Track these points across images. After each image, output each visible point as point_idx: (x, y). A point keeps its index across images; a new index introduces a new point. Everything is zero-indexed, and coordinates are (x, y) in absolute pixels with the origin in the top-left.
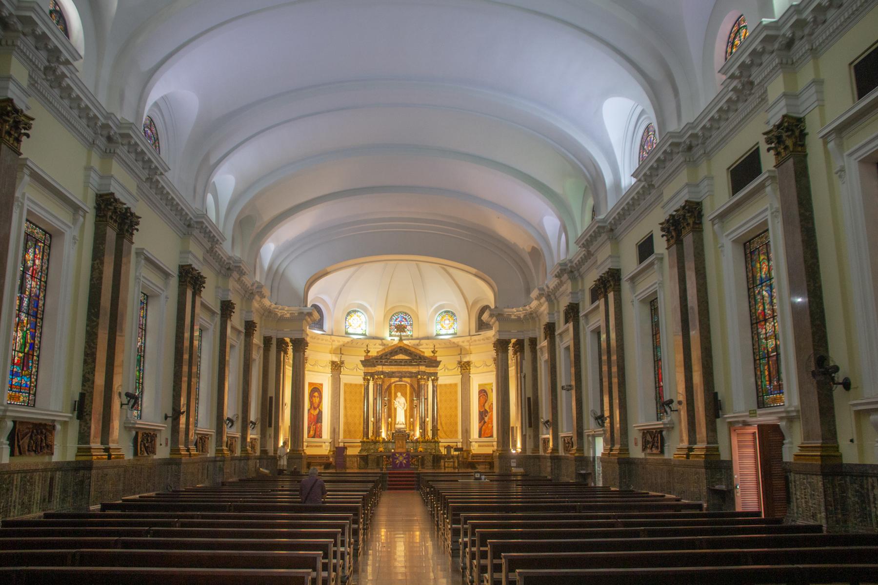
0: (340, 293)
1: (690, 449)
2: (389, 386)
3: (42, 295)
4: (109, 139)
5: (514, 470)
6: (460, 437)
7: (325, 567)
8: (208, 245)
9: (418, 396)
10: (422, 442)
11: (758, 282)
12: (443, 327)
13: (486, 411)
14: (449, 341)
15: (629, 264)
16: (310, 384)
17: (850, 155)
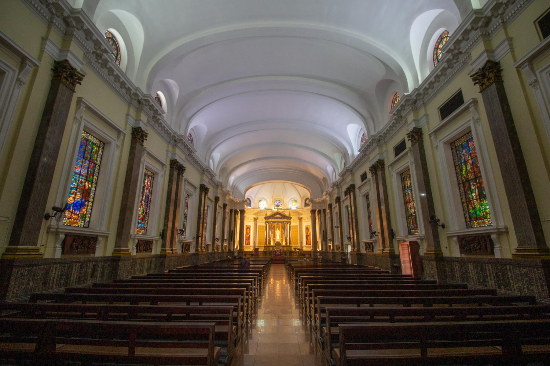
1: (383, 250)
2: (274, 226)
3: (150, 195)
4: (175, 141)
5: (319, 257)
6: (299, 244)
7: (247, 294)
8: (210, 177)
9: (284, 230)
11: (406, 188)
13: (308, 235)
14: (295, 210)
15: (358, 182)
16: (246, 226)
17: (440, 141)
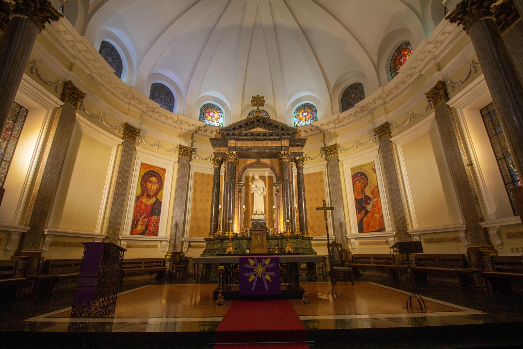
0: (192, 75)
10: (291, 238)
12: (301, 119)
13: (367, 199)
16: (143, 165)
